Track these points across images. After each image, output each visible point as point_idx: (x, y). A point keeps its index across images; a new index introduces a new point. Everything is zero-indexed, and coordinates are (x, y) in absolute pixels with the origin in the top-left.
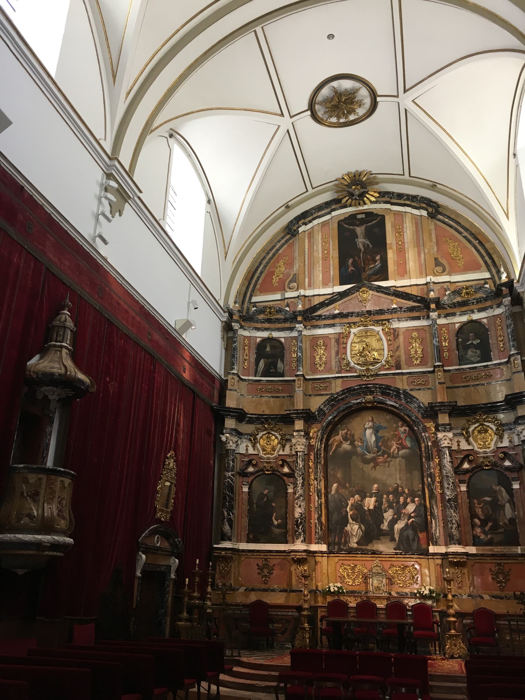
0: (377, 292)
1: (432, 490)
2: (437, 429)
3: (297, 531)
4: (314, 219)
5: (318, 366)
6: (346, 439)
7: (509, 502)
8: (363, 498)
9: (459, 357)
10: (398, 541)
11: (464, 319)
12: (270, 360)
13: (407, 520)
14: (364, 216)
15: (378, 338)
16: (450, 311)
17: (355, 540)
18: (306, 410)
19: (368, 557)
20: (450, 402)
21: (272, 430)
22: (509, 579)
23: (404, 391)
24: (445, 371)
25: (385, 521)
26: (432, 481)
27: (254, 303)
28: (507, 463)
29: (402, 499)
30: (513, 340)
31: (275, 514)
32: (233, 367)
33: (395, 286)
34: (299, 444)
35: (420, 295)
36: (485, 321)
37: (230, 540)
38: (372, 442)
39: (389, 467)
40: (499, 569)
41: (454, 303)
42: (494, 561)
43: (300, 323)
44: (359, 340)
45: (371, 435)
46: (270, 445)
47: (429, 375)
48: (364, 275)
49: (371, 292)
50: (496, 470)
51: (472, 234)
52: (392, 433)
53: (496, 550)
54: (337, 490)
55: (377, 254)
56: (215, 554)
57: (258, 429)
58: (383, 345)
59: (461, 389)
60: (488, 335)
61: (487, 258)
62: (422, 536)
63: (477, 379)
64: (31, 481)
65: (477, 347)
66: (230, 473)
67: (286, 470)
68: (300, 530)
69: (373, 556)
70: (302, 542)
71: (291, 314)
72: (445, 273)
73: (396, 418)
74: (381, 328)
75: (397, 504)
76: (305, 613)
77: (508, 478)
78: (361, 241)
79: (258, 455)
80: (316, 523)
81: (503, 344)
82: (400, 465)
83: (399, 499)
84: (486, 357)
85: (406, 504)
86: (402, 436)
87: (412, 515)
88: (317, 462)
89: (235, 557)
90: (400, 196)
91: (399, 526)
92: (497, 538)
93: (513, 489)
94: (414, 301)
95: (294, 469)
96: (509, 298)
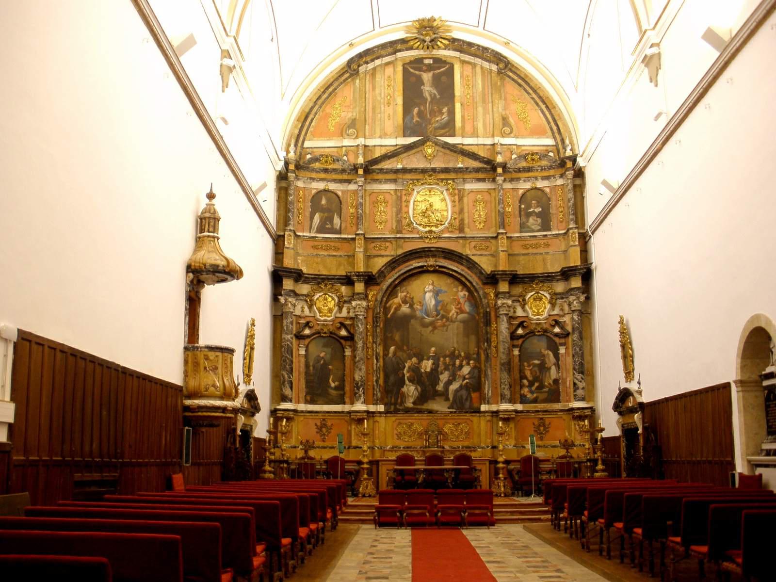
0: (443, 147)
1: (488, 354)
2: (497, 295)
3: (355, 394)
4: (378, 58)
5: (378, 224)
6: (405, 302)
7: (554, 364)
8: (421, 360)
9: (520, 224)
10: (453, 401)
11: (528, 185)
12: (326, 214)
13: (461, 382)
14: (431, 61)
15: (441, 198)
16: (515, 175)
17: (412, 400)
18: (369, 272)
19: (425, 416)
20: (512, 271)
21: (329, 291)
22: (548, 431)
23: (467, 256)
24: (508, 237)
25: (440, 383)
26: (488, 345)
27: (308, 148)
28: (557, 330)
29: (458, 362)
30: (573, 214)
31: (332, 377)
32: (290, 222)
33: (463, 145)
34: (359, 308)
35: (485, 156)
36: (548, 190)
37: (291, 401)
38: (432, 306)
39: (447, 330)
40: (541, 423)
41: (520, 168)
42: (538, 416)
43: (361, 177)
44: (422, 199)
45: (430, 298)
46: (327, 306)
47: (491, 240)
48: (430, 128)
49: (437, 148)
50: (547, 336)
51: (540, 97)
52: (452, 298)
53: (539, 407)
54: (395, 354)
55: (446, 105)
56: (278, 415)
57: (314, 291)
58: (446, 206)
59: (522, 258)
60: (550, 204)
61: (553, 124)
62: (474, 395)
63: (536, 246)
64: (211, 358)
65: (538, 215)
66: (289, 337)
67: (343, 333)
68: (361, 393)
69: (429, 415)
70: (362, 403)
71: (350, 165)
72: (512, 135)
73: (456, 283)
74: (445, 187)
75: (453, 366)
76: (365, 466)
77: (556, 343)
78: (428, 89)
79: (315, 317)
80: (374, 385)
81: (563, 215)
82: (458, 328)
83: (455, 362)
84: (546, 226)
85: (461, 366)
86: (462, 300)
87: (467, 376)
88: (377, 326)
89: (296, 417)
90: (470, 45)
91: (454, 386)
92: (542, 396)
93: (559, 353)
94: (480, 162)
95: (352, 331)
96: (573, 172)
